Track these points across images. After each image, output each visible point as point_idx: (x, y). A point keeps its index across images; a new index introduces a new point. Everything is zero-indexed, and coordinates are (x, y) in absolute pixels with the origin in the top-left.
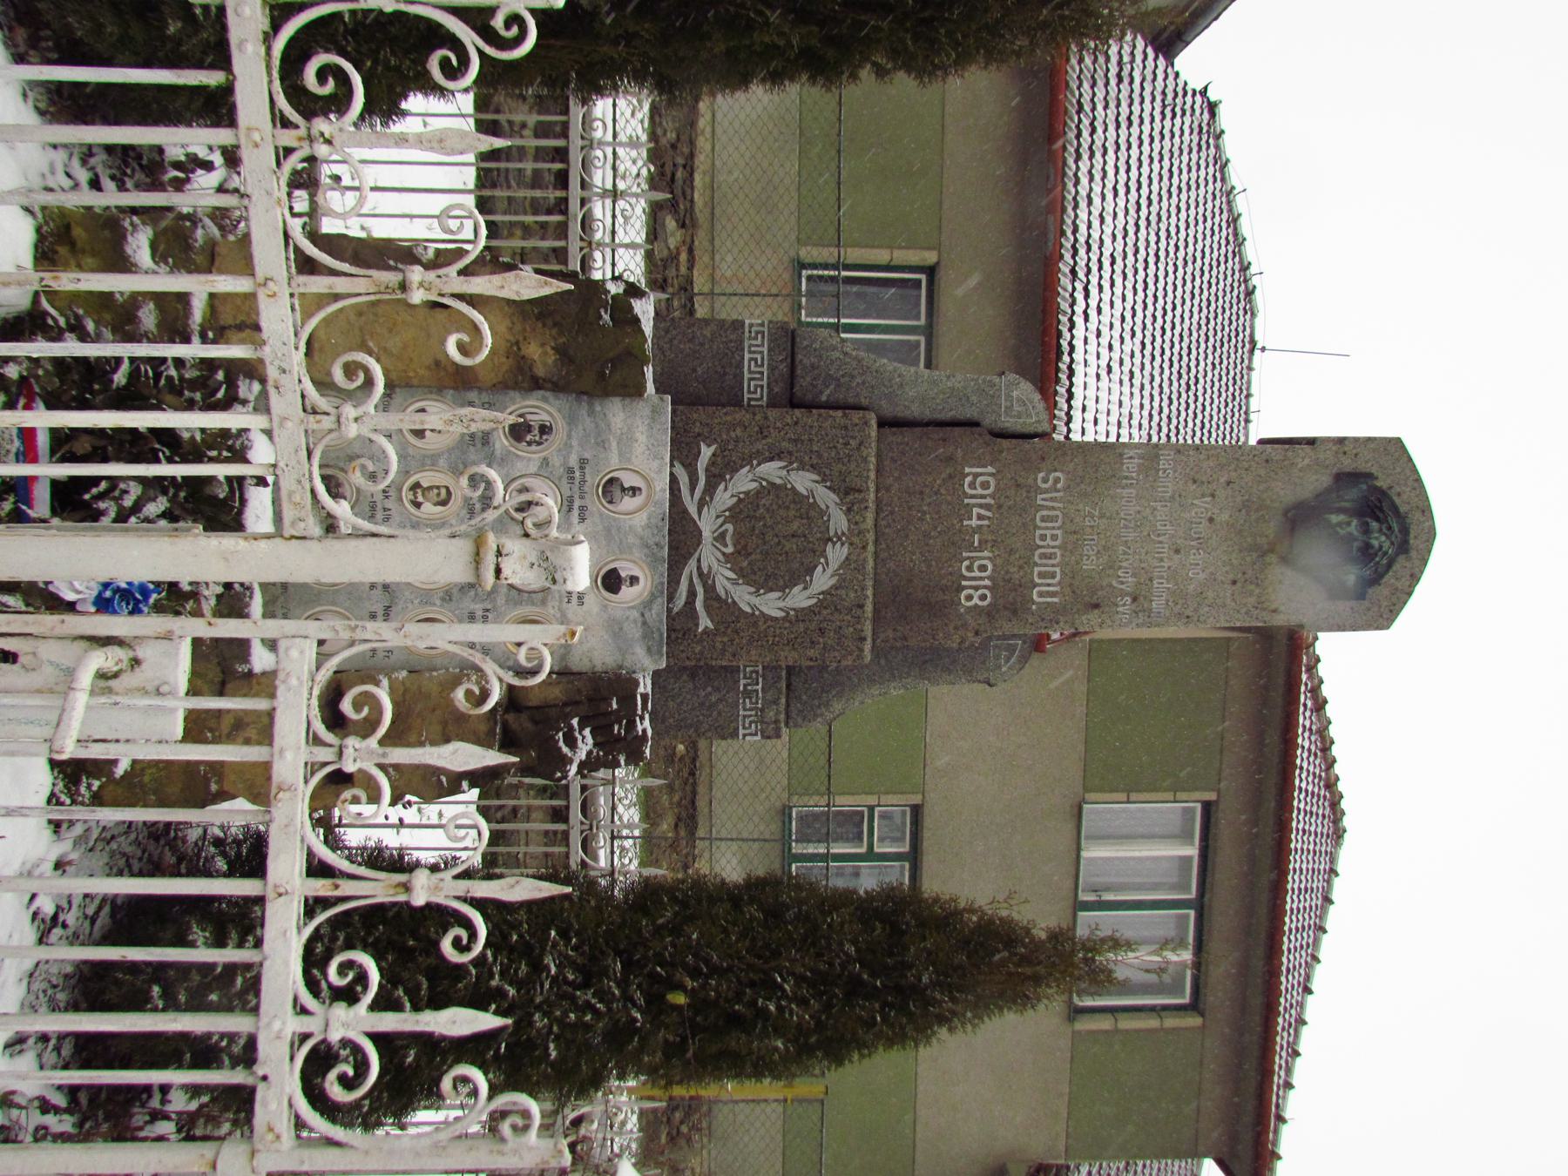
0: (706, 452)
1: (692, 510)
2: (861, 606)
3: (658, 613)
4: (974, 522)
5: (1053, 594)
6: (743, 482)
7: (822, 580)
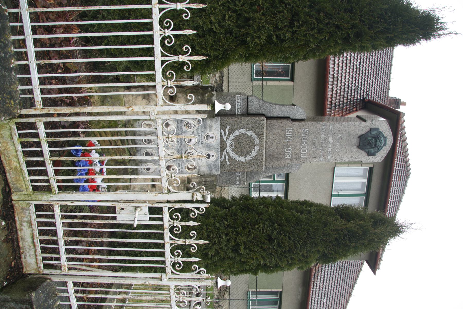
0: (228, 127)
1: (225, 139)
2: (262, 159)
3: (218, 163)
4: (288, 140)
5: (306, 155)
6: (236, 133)
7: (254, 154)
